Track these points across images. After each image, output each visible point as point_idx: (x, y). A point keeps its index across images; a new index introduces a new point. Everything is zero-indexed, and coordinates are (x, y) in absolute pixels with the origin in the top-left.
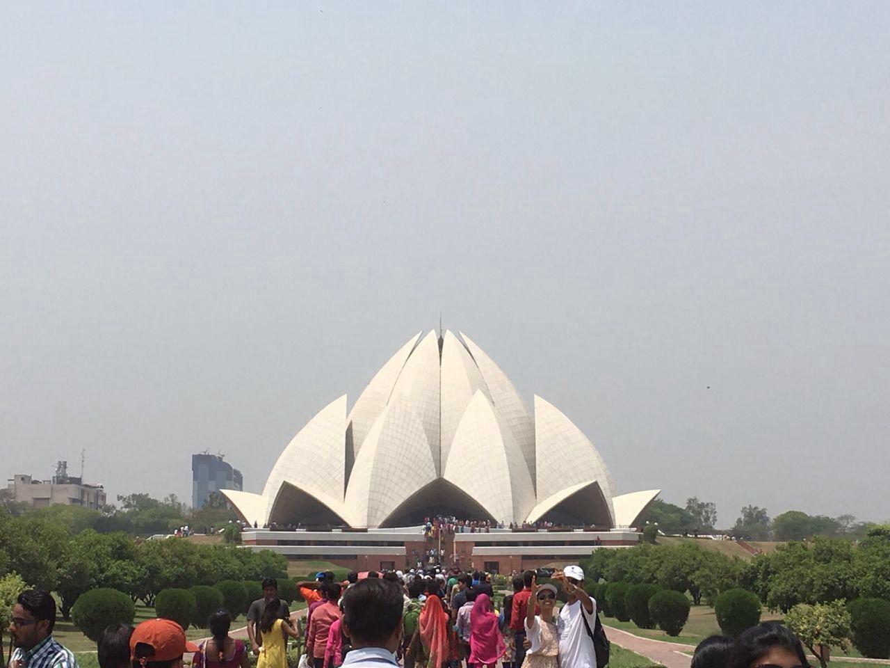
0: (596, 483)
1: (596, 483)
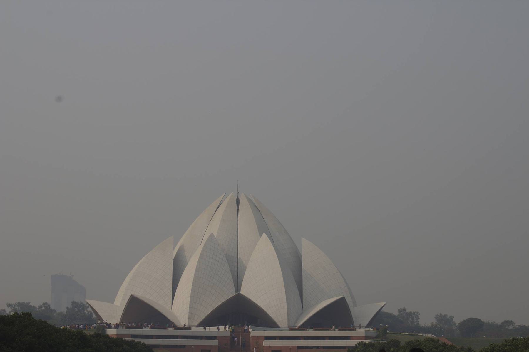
0: (344, 297)
1: (344, 297)
